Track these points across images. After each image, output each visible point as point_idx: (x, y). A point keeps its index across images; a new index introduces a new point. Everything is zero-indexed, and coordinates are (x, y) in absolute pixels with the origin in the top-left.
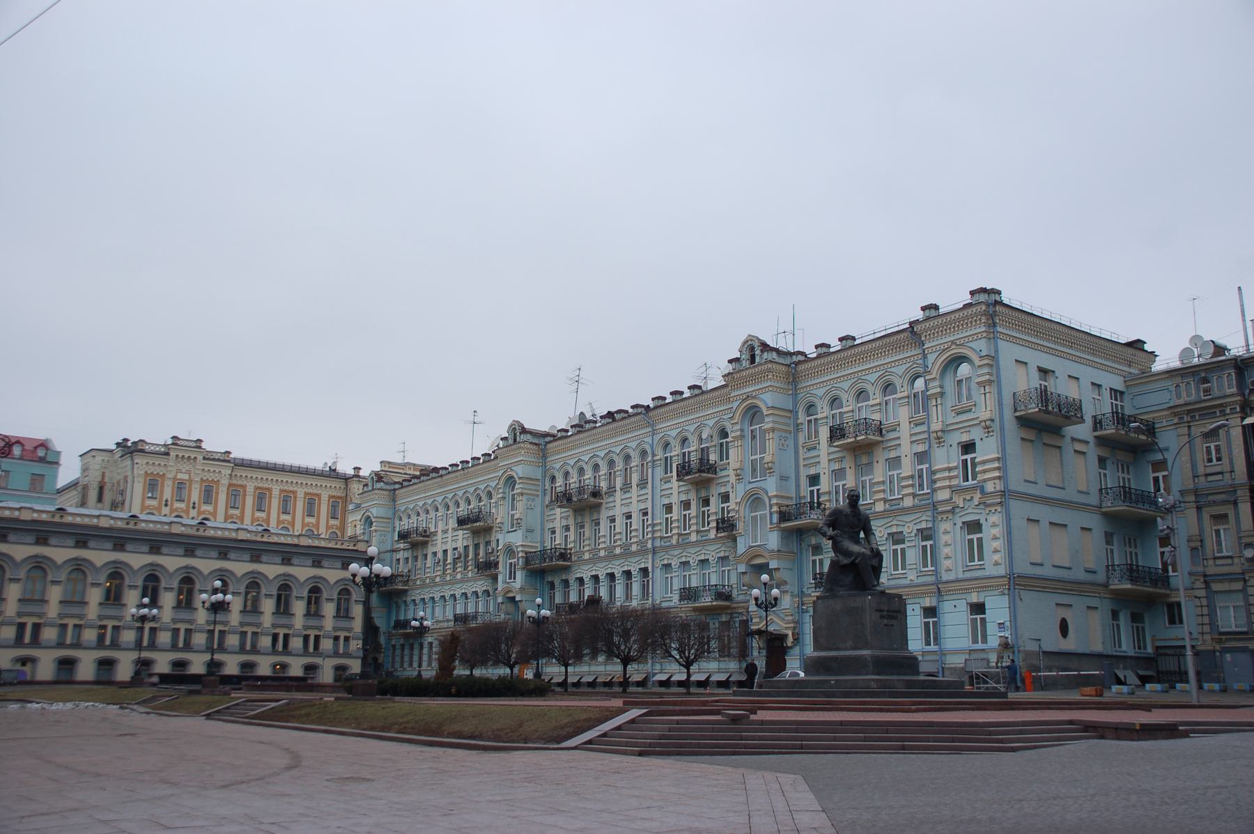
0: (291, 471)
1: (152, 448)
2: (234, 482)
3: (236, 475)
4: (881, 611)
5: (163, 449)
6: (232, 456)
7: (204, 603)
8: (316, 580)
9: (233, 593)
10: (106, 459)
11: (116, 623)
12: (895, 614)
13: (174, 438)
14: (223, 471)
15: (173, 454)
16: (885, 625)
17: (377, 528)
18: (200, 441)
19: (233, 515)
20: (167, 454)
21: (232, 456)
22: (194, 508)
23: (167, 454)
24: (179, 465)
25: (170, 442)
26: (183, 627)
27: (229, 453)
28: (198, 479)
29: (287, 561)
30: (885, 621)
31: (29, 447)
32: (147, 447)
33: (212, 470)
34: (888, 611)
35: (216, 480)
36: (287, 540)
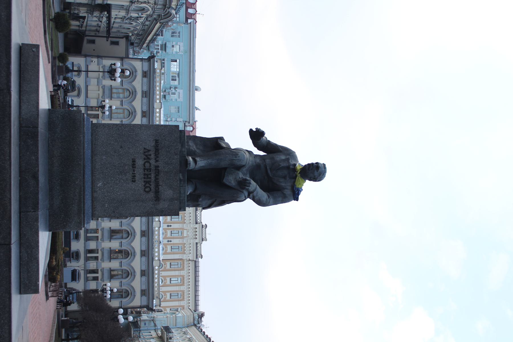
0: (195, 296)
1: (199, 218)
2: (186, 263)
3: (189, 263)
4: (157, 150)
5: (199, 221)
6: (200, 259)
7: (114, 64)
8: (133, 274)
9: (122, 81)
12: (153, 187)
13: (206, 225)
14: (191, 255)
15: (197, 226)
16: (134, 161)
17: (169, 318)
18: (206, 240)
19: (166, 296)
20: (196, 223)
21: (200, 259)
22: (168, 226)
23: (196, 223)
24: (191, 230)
25: (204, 224)
27: (202, 258)
28: (184, 242)
29: (143, 253)
30: (140, 162)
32: (199, 212)
33: (191, 248)
34: (157, 167)
35: (185, 252)
36: (156, 253)
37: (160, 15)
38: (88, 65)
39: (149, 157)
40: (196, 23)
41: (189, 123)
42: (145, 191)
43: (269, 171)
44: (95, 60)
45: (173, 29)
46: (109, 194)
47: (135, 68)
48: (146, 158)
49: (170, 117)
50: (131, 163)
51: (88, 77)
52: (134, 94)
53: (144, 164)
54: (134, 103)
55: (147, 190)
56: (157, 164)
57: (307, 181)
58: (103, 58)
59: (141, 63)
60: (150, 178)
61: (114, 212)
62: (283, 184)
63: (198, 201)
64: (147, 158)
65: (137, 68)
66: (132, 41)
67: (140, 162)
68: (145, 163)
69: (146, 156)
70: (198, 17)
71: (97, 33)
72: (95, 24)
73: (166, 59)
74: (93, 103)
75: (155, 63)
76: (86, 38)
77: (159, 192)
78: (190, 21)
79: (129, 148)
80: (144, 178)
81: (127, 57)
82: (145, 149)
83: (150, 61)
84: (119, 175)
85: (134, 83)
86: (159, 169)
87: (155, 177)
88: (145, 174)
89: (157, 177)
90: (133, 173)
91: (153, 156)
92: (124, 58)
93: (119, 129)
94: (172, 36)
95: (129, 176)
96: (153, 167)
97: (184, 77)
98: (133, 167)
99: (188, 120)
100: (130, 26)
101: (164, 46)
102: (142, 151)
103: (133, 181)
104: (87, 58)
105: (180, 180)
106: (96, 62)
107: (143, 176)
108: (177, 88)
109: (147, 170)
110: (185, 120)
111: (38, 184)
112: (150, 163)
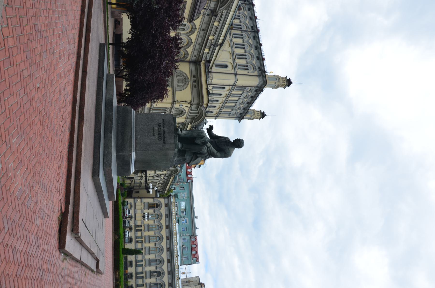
10: (197, 281)
11: (143, 241)
12: (162, 138)
16: (154, 128)
26: (144, 275)
30: (156, 128)
31: (196, 256)
37: (172, 172)
38: (135, 203)
39: (160, 126)
40: (192, 182)
41: (193, 236)
42: (159, 140)
43: (217, 143)
44: (139, 200)
45: (181, 186)
46: (143, 141)
47: (161, 202)
48: (159, 126)
49: (182, 233)
50: (152, 128)
51: (136, 209)
52: (161, 216)
53: (158, 129)
54: (161, 221)
55: (160, 139)
56: (164, 129)
57: (236, 148)
58: (144, 198)
59: (164, 199)
60: (161, 135)
61: (145, 148)
62: (224, 148)
63: (184, 156)
64: (159, 127)
65: (162, 202)
66: (159, 190)
67: (156, 128)
68: (158, 129)
69: (159, 126)
70: (193, 179)
71: (140, 187)
72: (138, 181)
73: (178, 202)
74: (139, 223)
75: (172, 199)
76: (134, 191)
77: (165, 140)
78: (189, 181)
79: (151, 123)
80: (158, 135)
81: (156, 197)
82: (158, 123)
83: (169, 198)
84: (147, 133)
85: (160, 211)
86: (164, 131)
87: (163, 134)
88: (159, 133)
89: (164, 134)
90: (153, 133)
91: (162, 126)
92: (155, 197)
93: (147, 115)
94: (181, 190)
95: (152, 134)
96: (162, 131)
97: (188, 212)
98: (153, 130)
99: (192, 235)
100: (157, 181)
101: (176, 195)
102: (157, 124)
103: (153, 136)
104: (135, 199)
105: (175, 136)
106: (140, 201)
107: (158, 134)
108: (185, 217)
109: (160, 131)
110: (191, 235)
111: (112, 123)
112: (161, 129)
